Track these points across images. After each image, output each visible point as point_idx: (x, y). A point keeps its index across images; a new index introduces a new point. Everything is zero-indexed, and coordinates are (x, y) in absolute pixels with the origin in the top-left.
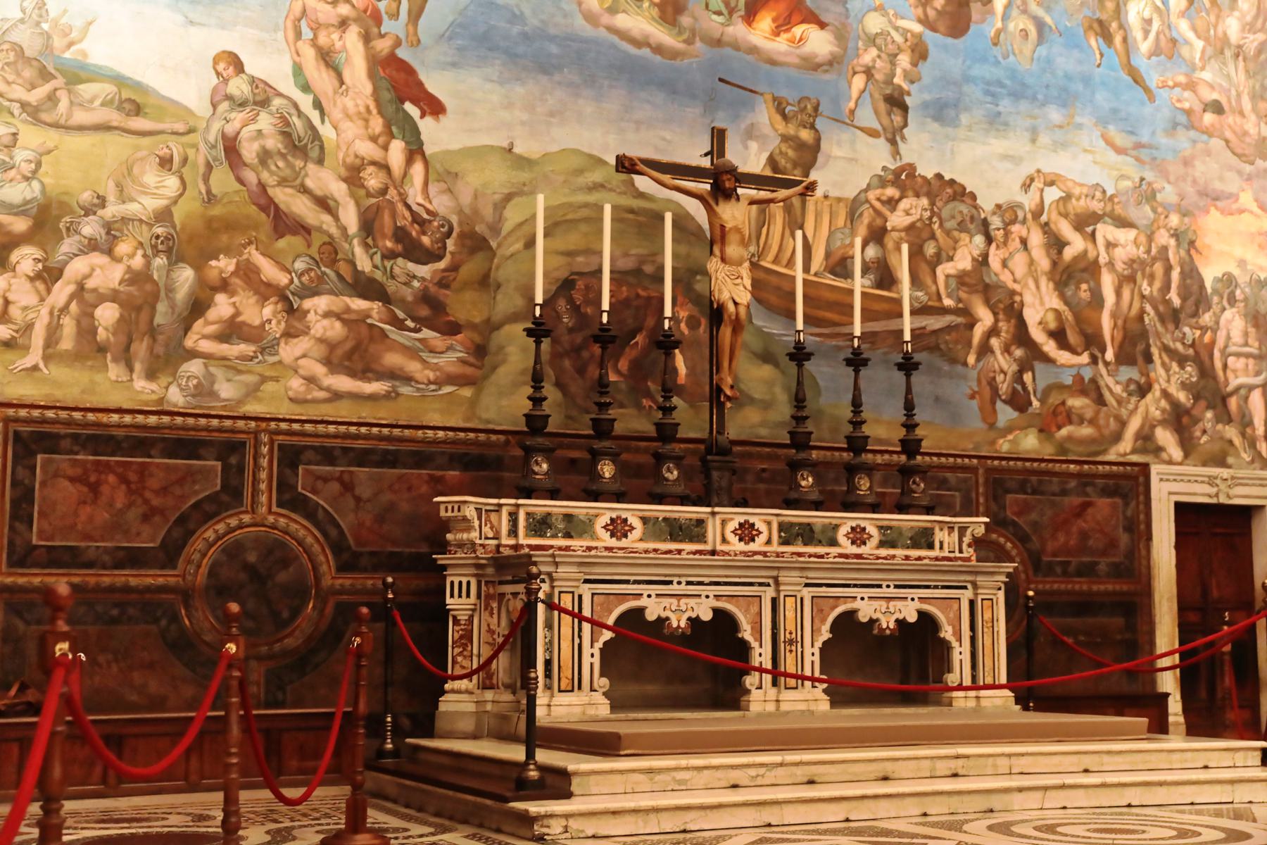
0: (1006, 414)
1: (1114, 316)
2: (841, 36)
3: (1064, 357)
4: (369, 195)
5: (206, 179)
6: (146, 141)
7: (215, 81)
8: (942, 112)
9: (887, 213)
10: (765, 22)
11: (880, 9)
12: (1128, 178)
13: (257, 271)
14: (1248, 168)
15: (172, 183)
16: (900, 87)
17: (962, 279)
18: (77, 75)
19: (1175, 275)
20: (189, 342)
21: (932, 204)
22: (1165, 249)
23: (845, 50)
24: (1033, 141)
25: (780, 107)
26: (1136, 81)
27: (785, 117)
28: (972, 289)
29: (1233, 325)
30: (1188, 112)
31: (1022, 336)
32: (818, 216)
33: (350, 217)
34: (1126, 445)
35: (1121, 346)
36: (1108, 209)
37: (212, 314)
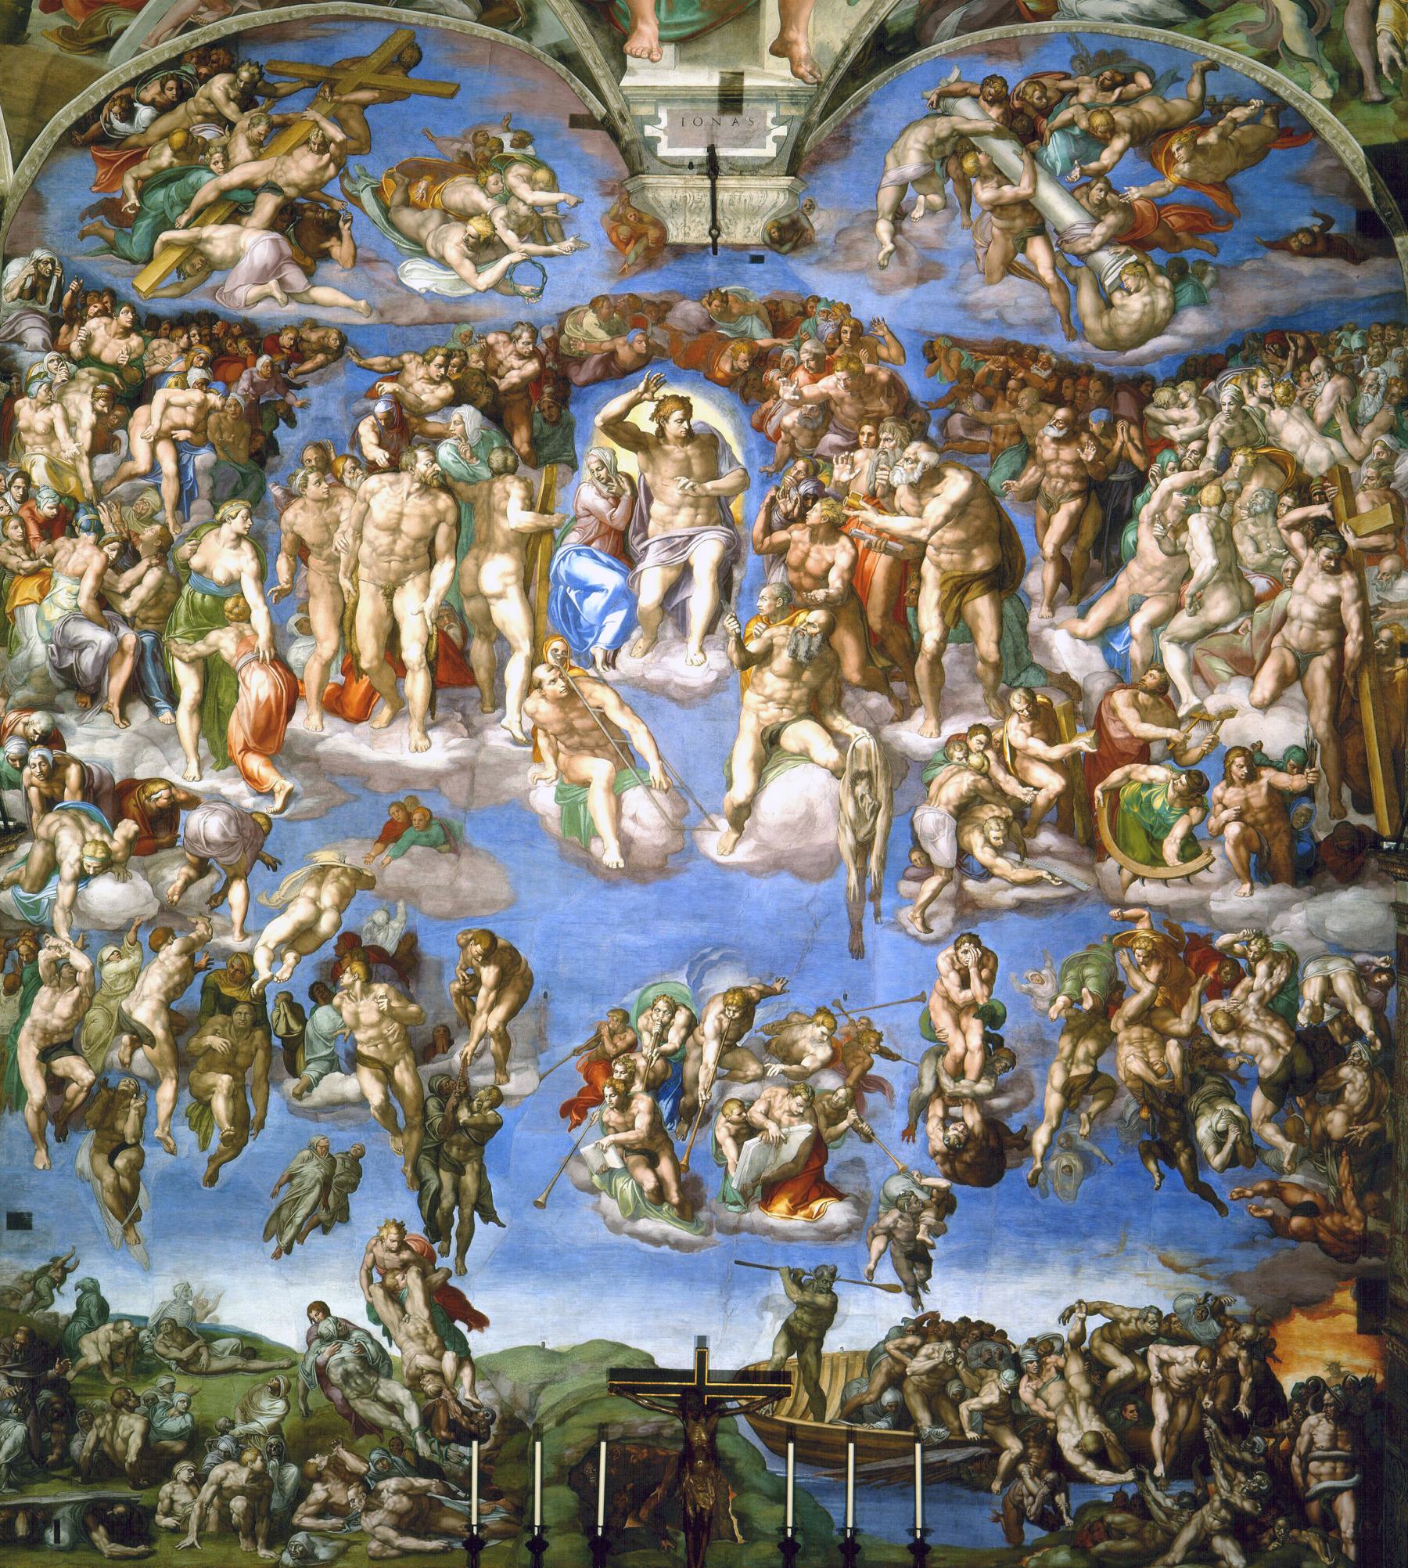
0: (1033, 1533)
1: (1166, 1431)
2: (860, 1204)
3: (1105, 1476)
4: (428, 1397)
5: (304, 1399)
6: (260, 1377)
7: (309, 1325)
8: (973, 1259)
9: (905, 1358)
10: (782, 1205)
11: (904, 1172)
12: (1191, 1296)
13: (343, 1463)
14: (1346, 1267)
15: (280, 1405)
16: (923, 1242)
17: (987, 1412)
18: (212, 1335)
19: (1245, 1387)
20: (296, 1521)
21: (957, 1345)
22: (1234, 1361)
23: (865, 1216)
24: (1075, 1273)
25: (795, 1277)
26: (1204, 1197)
27: (801, 1286)
28: (999, 1422)
29: (1319, 1428)
30: (1272, 1220)
31: (1055, 1459)
32: (834, 1370)
33: (413, 1416)
34: (1177, 1554)
35: (1176, 1458)
36: (1165, 1327)
37: (312, 1498)
